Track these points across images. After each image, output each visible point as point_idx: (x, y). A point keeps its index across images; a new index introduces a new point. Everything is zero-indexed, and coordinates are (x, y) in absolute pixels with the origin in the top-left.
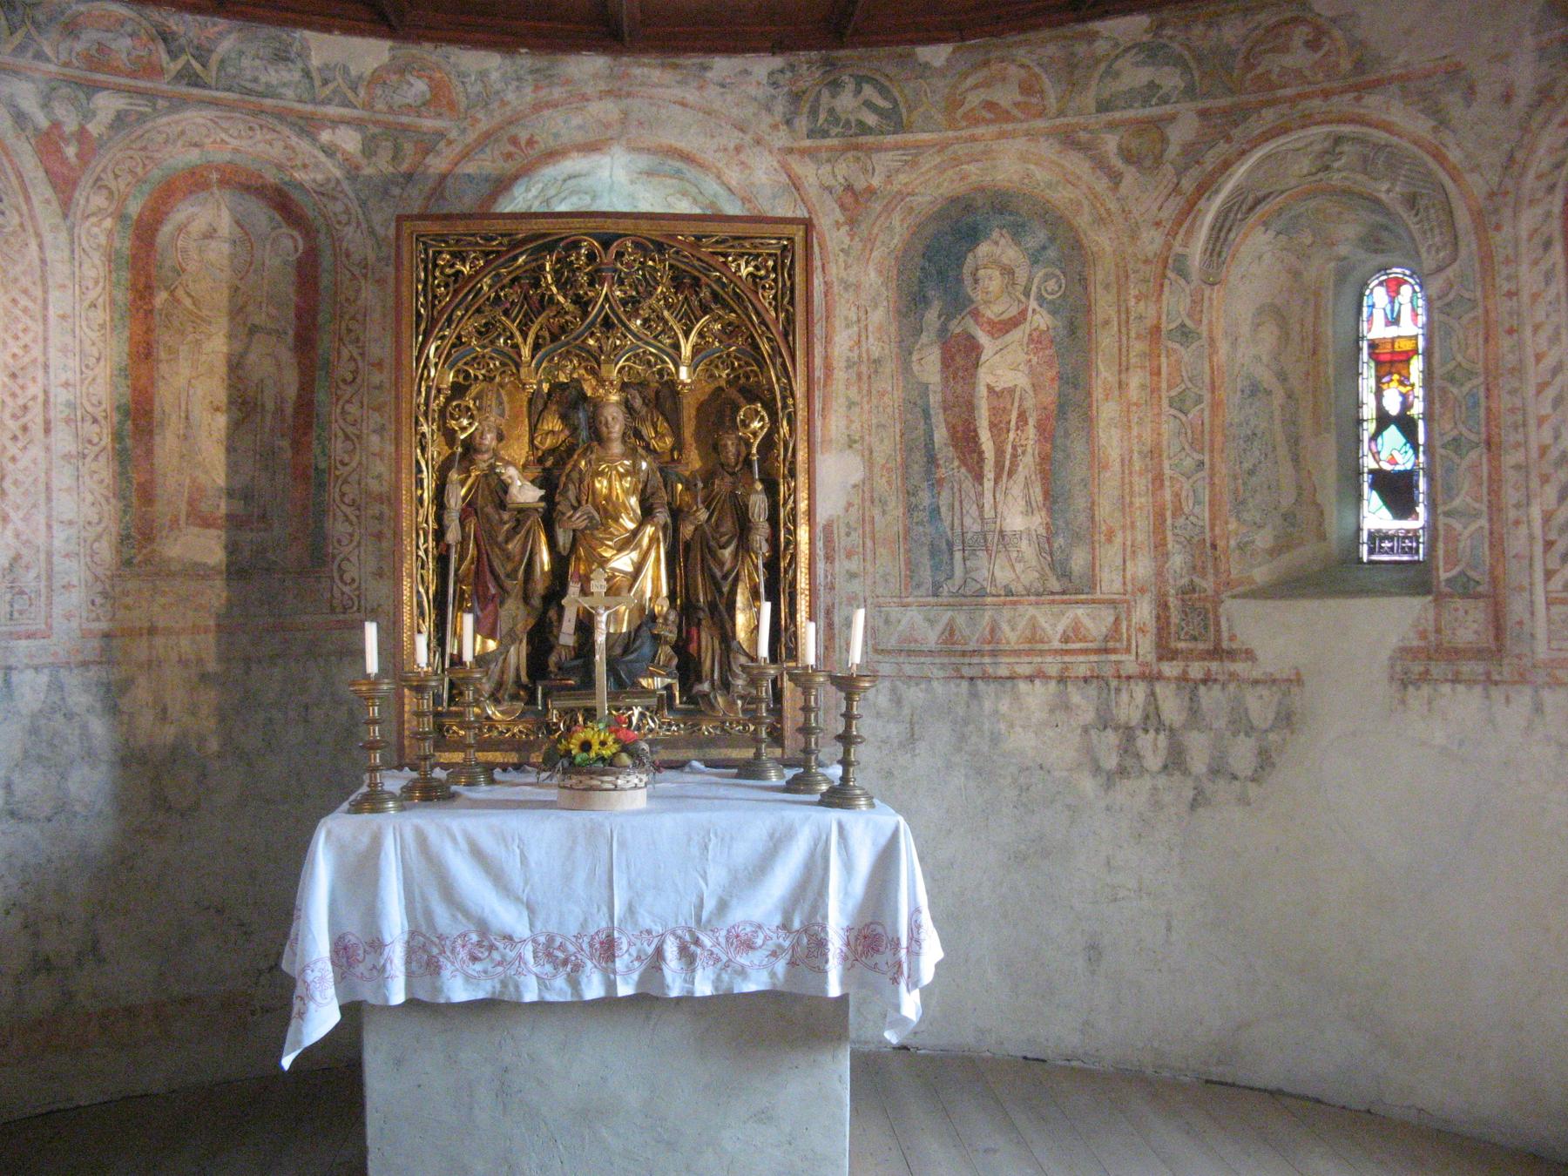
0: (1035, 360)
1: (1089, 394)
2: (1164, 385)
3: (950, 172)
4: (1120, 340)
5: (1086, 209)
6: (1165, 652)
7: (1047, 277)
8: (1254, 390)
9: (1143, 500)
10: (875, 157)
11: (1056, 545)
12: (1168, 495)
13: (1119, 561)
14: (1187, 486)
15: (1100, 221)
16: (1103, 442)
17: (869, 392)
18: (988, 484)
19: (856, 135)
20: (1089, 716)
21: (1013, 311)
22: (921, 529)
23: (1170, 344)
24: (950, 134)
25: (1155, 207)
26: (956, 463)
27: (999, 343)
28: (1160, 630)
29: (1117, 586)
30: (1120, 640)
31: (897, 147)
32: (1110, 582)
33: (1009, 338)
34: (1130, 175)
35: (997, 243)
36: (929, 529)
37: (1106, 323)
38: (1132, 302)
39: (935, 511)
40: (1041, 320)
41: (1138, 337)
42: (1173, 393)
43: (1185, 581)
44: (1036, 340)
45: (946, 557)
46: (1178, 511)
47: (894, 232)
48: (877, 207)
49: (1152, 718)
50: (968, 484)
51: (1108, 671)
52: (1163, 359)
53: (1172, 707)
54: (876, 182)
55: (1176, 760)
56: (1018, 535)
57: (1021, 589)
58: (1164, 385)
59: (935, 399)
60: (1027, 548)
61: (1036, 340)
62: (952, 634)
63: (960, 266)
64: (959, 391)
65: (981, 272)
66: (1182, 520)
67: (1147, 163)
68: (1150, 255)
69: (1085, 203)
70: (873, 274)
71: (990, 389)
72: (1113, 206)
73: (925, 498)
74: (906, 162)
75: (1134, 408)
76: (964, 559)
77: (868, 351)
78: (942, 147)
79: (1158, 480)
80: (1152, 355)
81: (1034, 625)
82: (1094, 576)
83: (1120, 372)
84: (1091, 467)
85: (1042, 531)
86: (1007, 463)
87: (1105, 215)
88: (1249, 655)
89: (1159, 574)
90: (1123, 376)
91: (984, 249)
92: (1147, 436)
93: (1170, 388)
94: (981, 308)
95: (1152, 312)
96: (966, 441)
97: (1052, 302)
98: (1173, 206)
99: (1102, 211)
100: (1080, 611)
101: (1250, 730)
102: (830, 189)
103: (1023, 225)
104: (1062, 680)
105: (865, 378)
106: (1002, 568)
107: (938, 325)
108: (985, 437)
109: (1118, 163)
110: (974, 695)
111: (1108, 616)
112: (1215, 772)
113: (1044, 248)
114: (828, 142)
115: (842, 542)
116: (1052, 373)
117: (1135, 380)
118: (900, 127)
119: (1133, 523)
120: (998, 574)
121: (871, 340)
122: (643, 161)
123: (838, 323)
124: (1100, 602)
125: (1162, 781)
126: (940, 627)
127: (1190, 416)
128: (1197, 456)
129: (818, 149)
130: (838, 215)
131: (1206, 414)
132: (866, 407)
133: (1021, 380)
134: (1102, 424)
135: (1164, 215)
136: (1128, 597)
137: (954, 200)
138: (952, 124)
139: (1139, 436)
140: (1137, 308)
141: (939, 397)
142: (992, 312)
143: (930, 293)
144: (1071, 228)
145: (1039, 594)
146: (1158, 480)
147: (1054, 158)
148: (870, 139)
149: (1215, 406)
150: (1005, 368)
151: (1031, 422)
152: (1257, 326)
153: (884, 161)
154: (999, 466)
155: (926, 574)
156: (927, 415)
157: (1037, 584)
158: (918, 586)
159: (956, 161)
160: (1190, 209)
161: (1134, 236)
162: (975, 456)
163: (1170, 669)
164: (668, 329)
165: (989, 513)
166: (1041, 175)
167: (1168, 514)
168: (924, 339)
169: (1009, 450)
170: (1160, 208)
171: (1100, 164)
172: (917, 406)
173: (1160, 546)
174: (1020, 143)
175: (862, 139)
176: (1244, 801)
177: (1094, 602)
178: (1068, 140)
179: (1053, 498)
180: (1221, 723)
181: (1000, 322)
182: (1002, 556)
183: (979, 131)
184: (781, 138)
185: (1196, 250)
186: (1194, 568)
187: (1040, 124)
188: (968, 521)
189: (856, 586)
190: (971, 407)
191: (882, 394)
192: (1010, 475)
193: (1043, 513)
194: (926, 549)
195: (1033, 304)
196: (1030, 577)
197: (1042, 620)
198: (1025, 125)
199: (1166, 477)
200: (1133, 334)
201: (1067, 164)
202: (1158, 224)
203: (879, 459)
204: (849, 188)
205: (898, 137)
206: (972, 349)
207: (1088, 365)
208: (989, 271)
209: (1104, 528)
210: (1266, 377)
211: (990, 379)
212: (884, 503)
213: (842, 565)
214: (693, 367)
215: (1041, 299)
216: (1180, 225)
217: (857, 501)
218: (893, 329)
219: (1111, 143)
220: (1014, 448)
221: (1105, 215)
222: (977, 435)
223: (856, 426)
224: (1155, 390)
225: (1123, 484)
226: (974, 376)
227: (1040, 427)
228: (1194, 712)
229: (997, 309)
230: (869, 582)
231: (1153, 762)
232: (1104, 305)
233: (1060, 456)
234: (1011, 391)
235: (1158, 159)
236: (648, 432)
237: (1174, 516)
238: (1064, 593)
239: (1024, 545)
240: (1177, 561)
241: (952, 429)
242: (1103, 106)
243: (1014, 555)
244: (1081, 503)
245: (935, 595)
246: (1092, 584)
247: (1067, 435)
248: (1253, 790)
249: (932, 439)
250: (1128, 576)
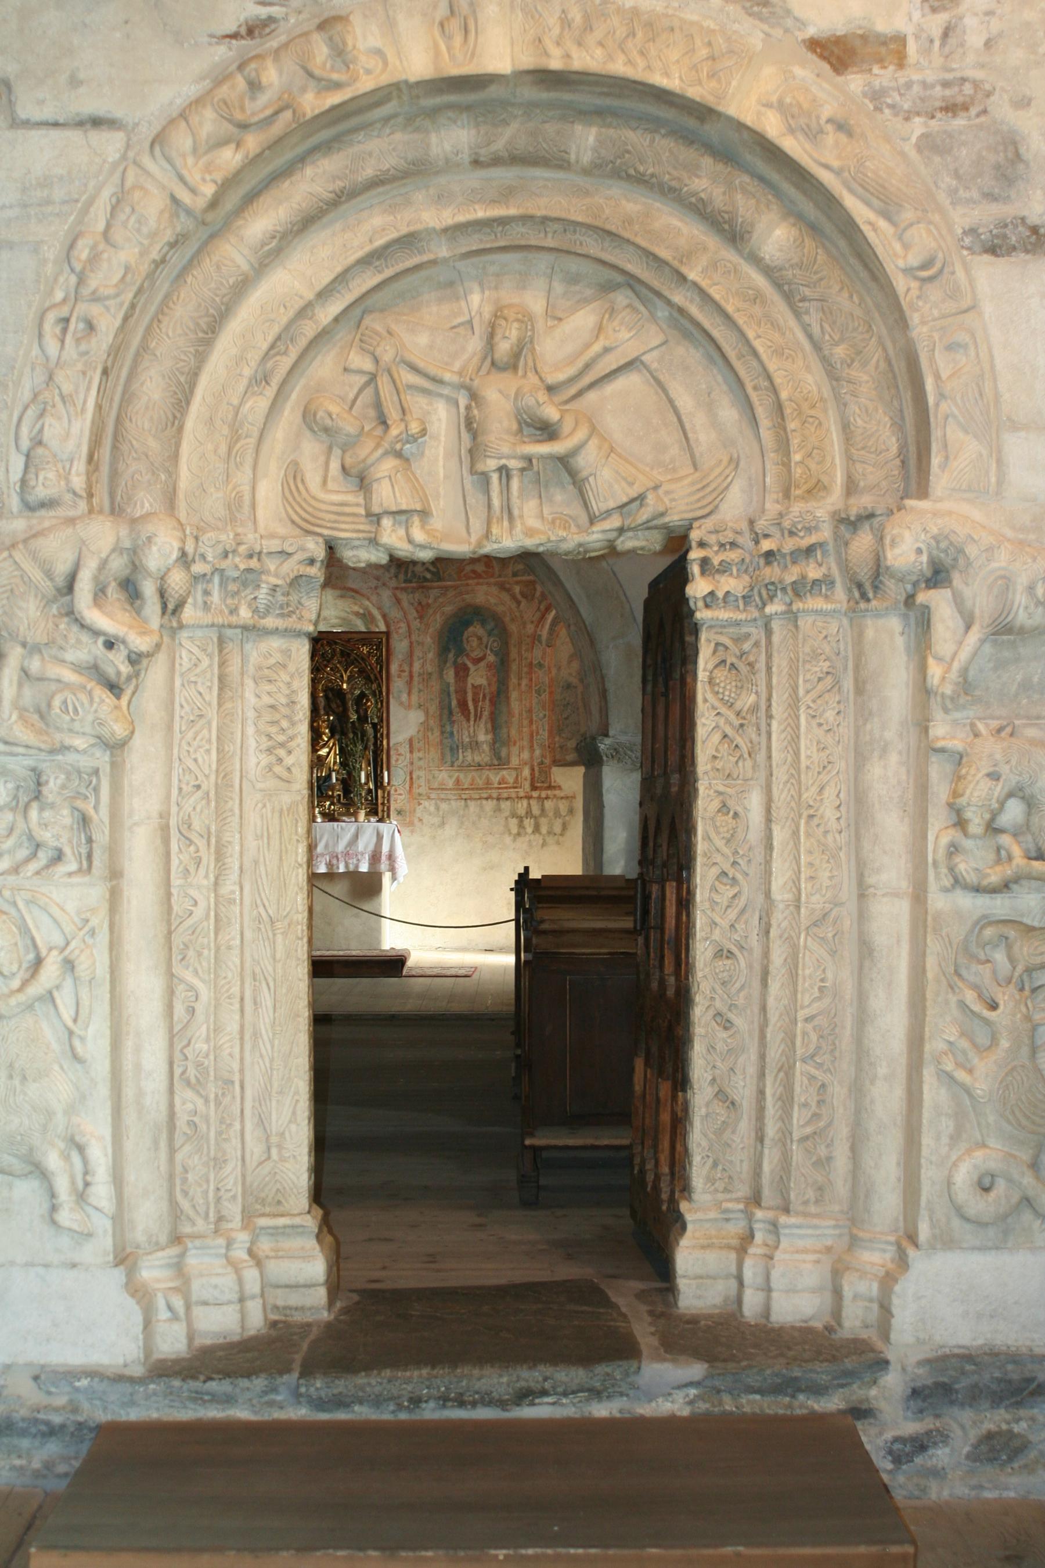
6: (534, 788)
8: (569, 686)
15: (513, 620)
20: (507, 813)
34: (524, 602)
39: (452, 734)
40: (491, 658)
44: (489, 666)
47: (437, 621)
48: (431, 611)
49: (529, 813)
51: (513, 795)
53: (536, 810)
55: (537, 829)
59: (452, 689)
60: (485, 747)
73: (448, 728)
78: (455, 587)
79: (531, 722)
80: (530, 673)
81: (488, 778)
88: (560, 788)
89: (532, 758)
91: (471, 629)
96: (463, 705)
98: (538, 615)
100: (505, 772)
101: (560, 816)
104: (498, 799)
109: (519, 597)
110: (466, 806)
111: (514, 774)
112: (549, 833)
115: (416, 745)
117: (524, 682)
118: (440, 579)
122: (338, 592)
123: (415, 658)
125: (532, 837)
130: (415, 614)
138: (460, 579)
140: (525, 655)
142: (474, 655)
145: (490, 766)
149: (551, 693)
152: (570, 662)
153: (434, 593)
155: (448, 758)
159: (461, 594)
160: (543, 617)
163: (535, 794)
164: (339, 671)
166: (493, 601)
171: (514, 597)
172: (445, 692)
173: (532, 747)
174: (485, 587)
176: (558, 843)
178: (502, 587)
180: (551, 814)
183: (470, 582)
184: (393, 583)
185: (544, 633)
187: (492, 580)
189: (421, 763)
190: (465, 693)
196: (487, 759)
203: (431, 712)
204: (420, 603)
206: (467, 669)
210: (574, 681)
213: (416, 755)
214: (348, 683)
219: (517, 589)
224: (530, 687)
227: (491, 700)
228: (543, 810)
231: (530, 830)
232: (514, 653)
236: (334, 706)
240: (538, 752)
241: (459, 701)
242: (515, 574)
246: (509, 763)
248: (561, 839)
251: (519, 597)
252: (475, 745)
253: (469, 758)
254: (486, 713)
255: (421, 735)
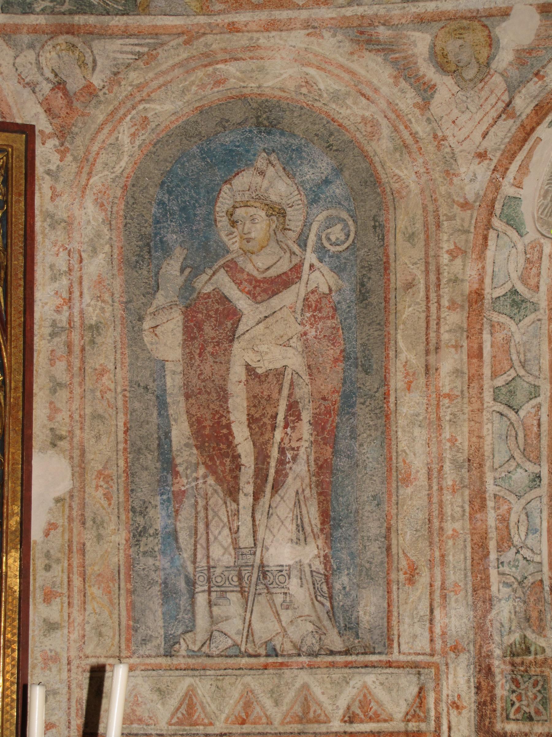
0: (312, 333)
1: (385, 381)
2: (487, 371)
3: (200, 73)
4: (428, 308)
5: (385, 130)
7: (330, 222)
9: (457, 525)
10: (97, 45)
11: (337, 586)
12: (491, 518)
13: (423, 608)
14: (517, 506)
16: (403, 445)
17: (82, 369)
18: (246, 501)
19: (71, 13)
21: (284, 266)
22: (151, 561)
23: (496, 317)
24: (202, 19)
25: (477, 136)
26: (202, 471)
27: (263, 309)
28: (481, 705)
29: (423, 644)
30: (425, 719)
31: (126, 33)
32: (412, 639)
33: (275, 302)
34: (446, 86)
35: (262, 173)
36: (163, 562)
37: (410, 286)
38: (445, 258)
40: (320, 278)
41: (453, 305)
42: (500, 382)
43: (516, 637)
44: (313, 305)
45: (184, 601)
46: (505, 541)
50: (217, 500)
52: (486, 336)
54: (97, 80)
56: (285, 572)
57: (288, 647)
58: (487, 371)
59: (173, 382)
61: (313, 305)
62: (191, 707)
63: (213, 202)
64: (207, 370)
65: (240, 212)
66: (510, 554)
67: (470, 73)
68: (471, 197)
69: (384, 122)
70: (90, 207)
71: (250, 370)
72: (421, 128)
73: (159, 519)
74: (140, 55)
75: (446, 401)
76: (210, 604)
77: (82, 312)
78: (189, 36)
79: (478, 502)
81: (306, 698)
82: (389, 627)
83: (427, 352)
84: (387, 480)
85: (318, 566)
86: (272, 471)
87: (410, 140)
90: (432, 358)
91: (244, 180)
92: (463, 441)
93: (494, 375)
94: (241, 261)
95: (471, 271)
96: (214, 440)
97: (337, 255)
98: (506, 129)
99: (406, 134)
100: (371, 679)
102: (33, 87)
103: (299, 150)
105: (77, 350)
106: (262, 616)
107: (180, 280)
108: (241, 434)
109: (430, 73)
111: (409, 686)
113: (327, 182)
114: (31, 20)
116: (333, 352)
117: (449, 362)
119: (443, 556)
120: (257, 626)
121: (87, 298)
124: (400, 666)
126: (173, 702)
127: (522, 413)
128: (532, 468)
129: (17, 29)
131: (545, 410)
132: (77, 390)
133: (294, 360)
134: (402, 422)
135: (489, 144)
136: (436, 659)
137: (201, 111)
139: (453, 440)
140: (451, 267)
141: (179, 380)
143: (171, 238)
144: (365, 156)
145: (316, 655)
146: (478, 502)
147: (342, 60)
148: (92, 20)
150: (272, 342)
151: (306, 416)
154: (260, 475)
155: (155, 623)
156: (162, 404)
157: (311, 641)
158: (145, 641)
159: (209, 59)
161: (449, 174)
162: (228, 461)
165: (246, 540)
166: (324, 83)
167: (492, 545)
168: (160, 299)
169: (275, 453)
170: (485, 135)
171: (405, 71)
172: (148, 389)
173: (481, 586)
174: (298, 39)
175: (79, 19)
177: (389, 665)
179: (333, 521)
181: (265, 280)
182: (262, 599)
186: (528, 619)
188: (216, 552)
190: (223, 395)
191: (102, 372)
192: (275, 488)
193: (320, 542)
194: (157, 588)
195: (311, 257)
196: (301, 630)
197: (317, 691)
198: (304, 14)
199: (489, 495)
200: (445, 302)
201: (362, 71)
202: (482, 156)
203: (95, 464)
204: (60, 85)
205: (131, 21)
207: (385, 342)
208: (252, 211)
209: (404, 563)
211: (250, 358)
212: (99, 524)
215: (321, 251)
216: (513, 156)
217: (62, 521)
218: (118, 284)
219: (420, 43)
220: (282, 451)
221: (410, 140)
222: (231, 433)
223: (63, 416)
224: (475, 378)
225: (430, 502)
226: (227, 352)
227: (318, 424)
229: (262, 261)
230: (75, 636)
232: (407, 261)
233: (342, 463)
234: (279, 374)
235: (486, 66)
237: (500, 549)
238: (347, 652)
239: (294, 584)
240: (504, 610)
241: (197, 424)
243: (279, 599)
244: (373, 528)
245: (168, 654)
246: (388, 640)
247: (354, 435)
249: (167, 435)
250: (438, 630)
251: (430, 73)
252: (255, 579)
253: (234, 626)
254: (300, 471)
255: (57, 540)
